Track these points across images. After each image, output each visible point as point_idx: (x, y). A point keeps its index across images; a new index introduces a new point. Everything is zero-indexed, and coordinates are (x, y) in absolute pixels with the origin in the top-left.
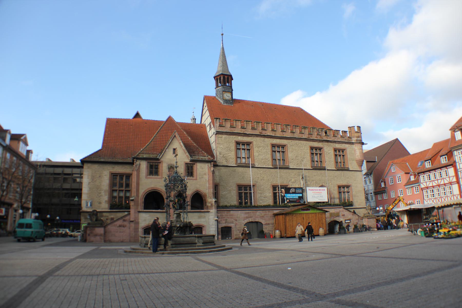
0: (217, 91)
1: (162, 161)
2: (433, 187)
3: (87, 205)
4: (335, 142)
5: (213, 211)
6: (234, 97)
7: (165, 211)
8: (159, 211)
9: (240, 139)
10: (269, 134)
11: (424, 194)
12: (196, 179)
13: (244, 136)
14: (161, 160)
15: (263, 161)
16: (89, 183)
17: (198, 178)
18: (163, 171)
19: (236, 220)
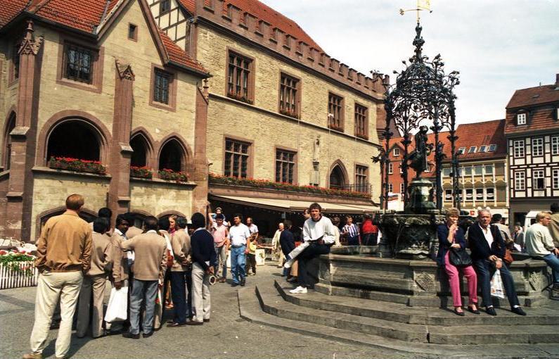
9: (237, 47)
15: (267, 99)
17: (177, 108)
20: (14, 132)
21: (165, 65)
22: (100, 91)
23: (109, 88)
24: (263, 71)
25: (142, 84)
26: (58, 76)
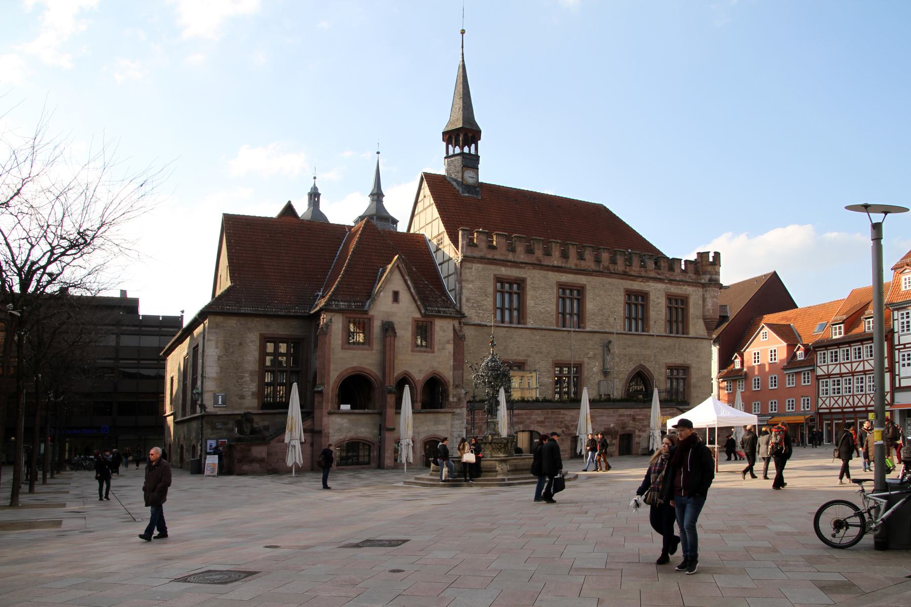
0: (449, 165)
1: (373, 316)
2: (841, 375)
4: (671, 281)
6: (480, 181)
7: (376, 411)
8: (366, 410)
9: (504, 271)
10: (556, 263)
11: (821, 388)
12: (433, 352)
13: (511, 267)
14: (371, 313)
17: (436, 349)
20: (316, 389)
21: (424, 316)
22: (372, 349)
23: (377, 346)
24: (535, 289)
25: (405, 333)
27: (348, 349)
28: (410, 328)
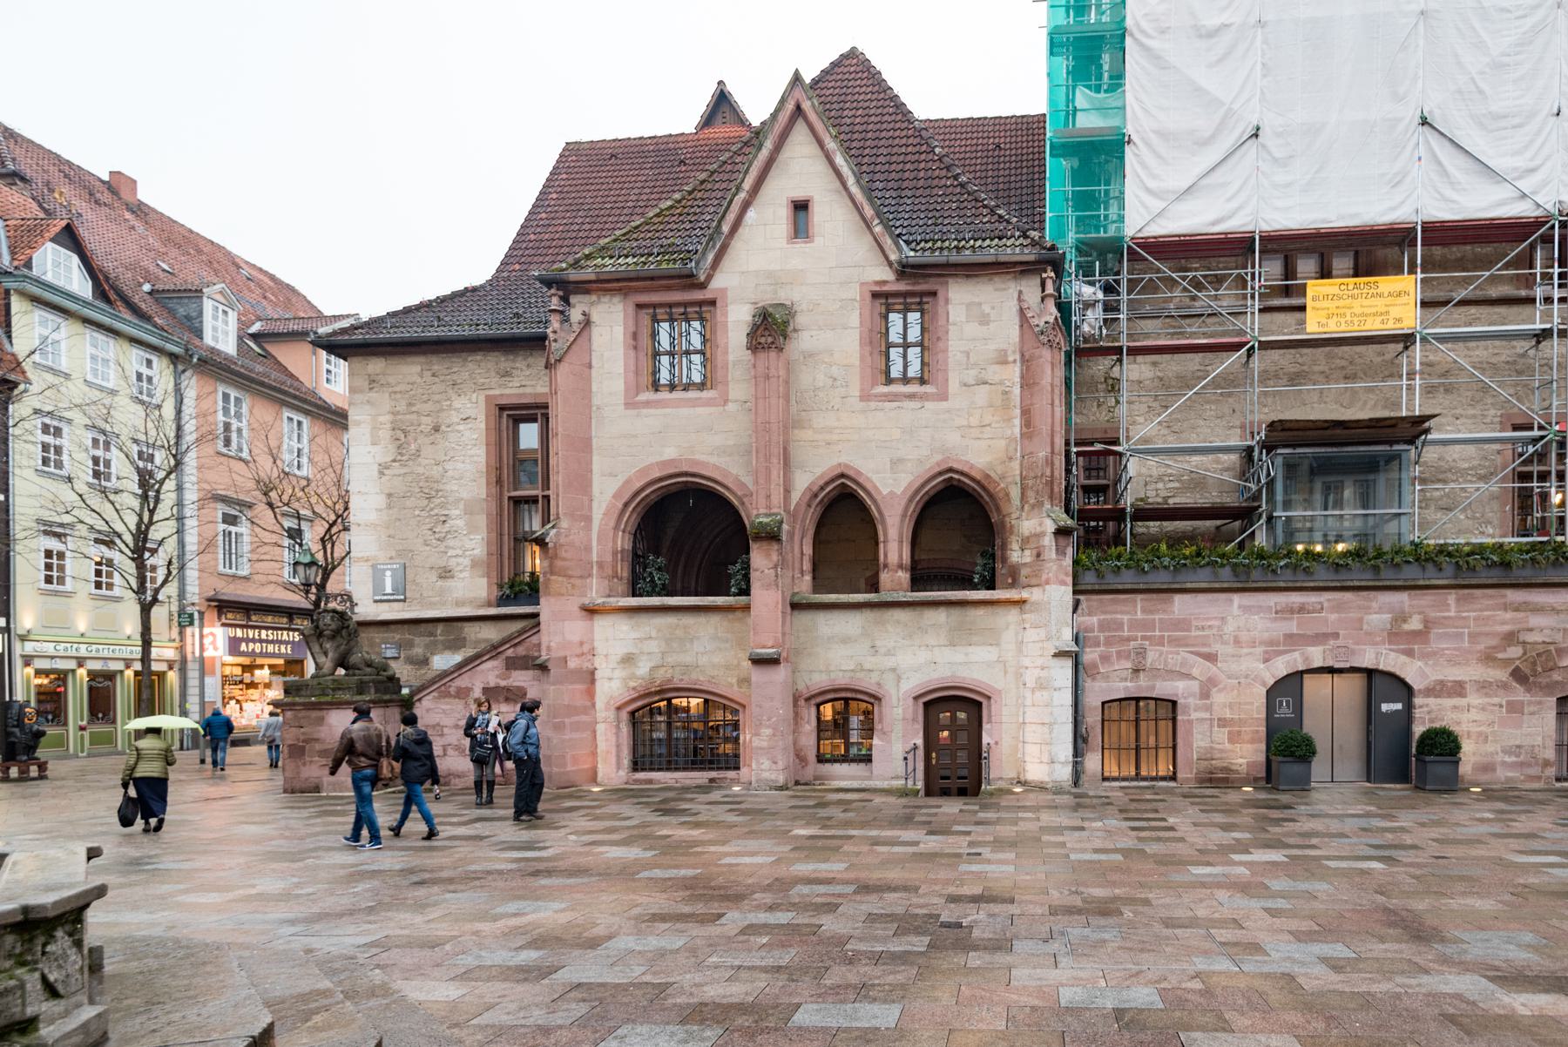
3: (378, 585)
5: (1053, 594)
12: (943, 396)
16: (383, 469)
17: (953, 386)
18: (731, 358)
19: (1211, 658)
23: (739, 387)
26: (627, 390)
27: (648, 404)
28: (854, 319)
